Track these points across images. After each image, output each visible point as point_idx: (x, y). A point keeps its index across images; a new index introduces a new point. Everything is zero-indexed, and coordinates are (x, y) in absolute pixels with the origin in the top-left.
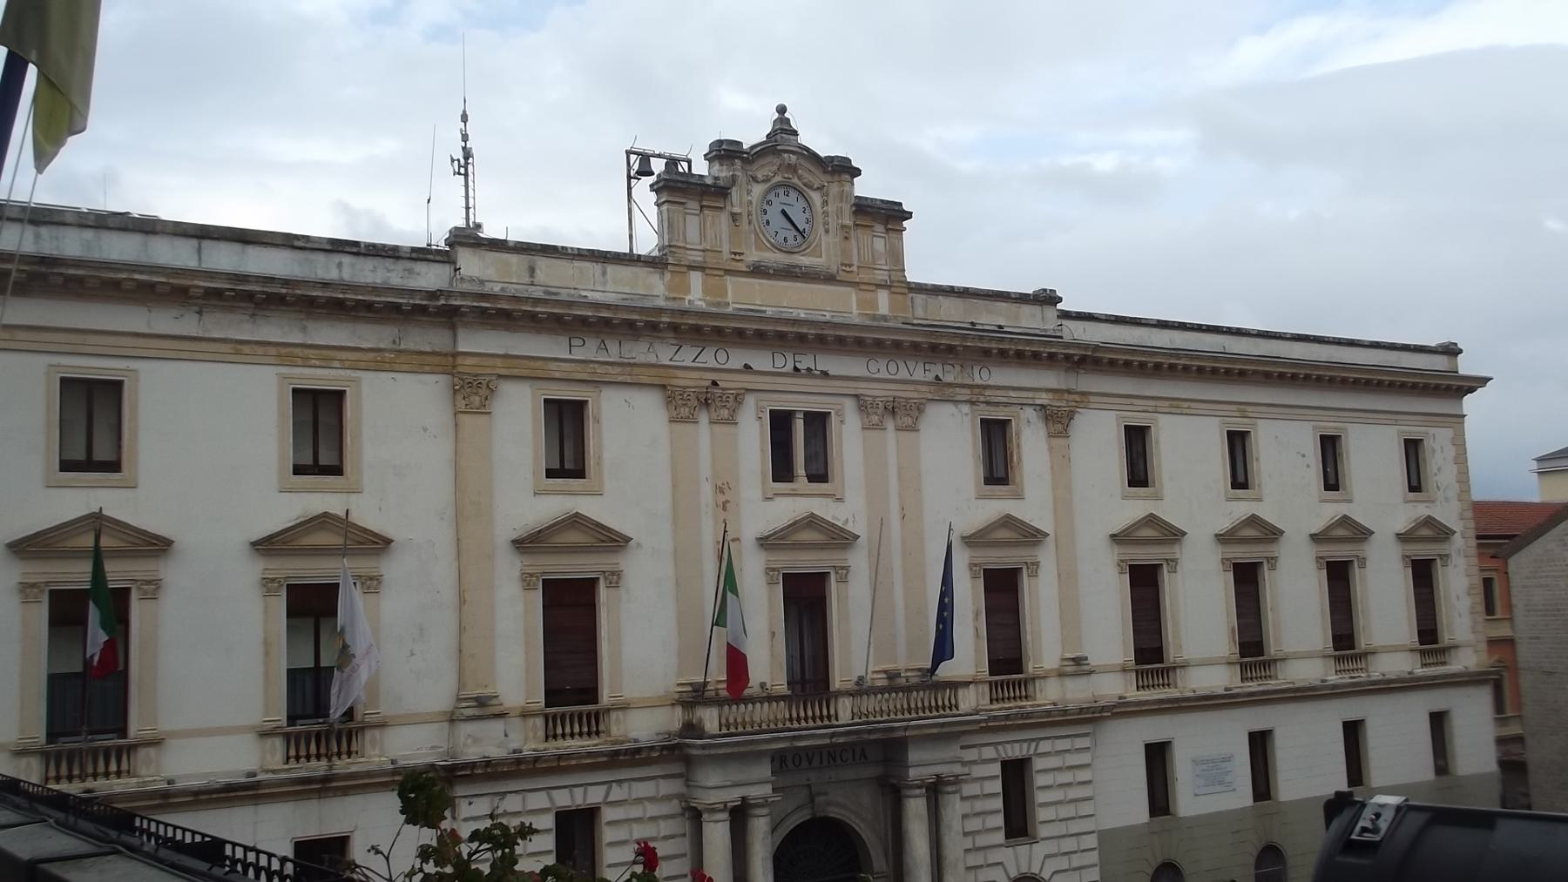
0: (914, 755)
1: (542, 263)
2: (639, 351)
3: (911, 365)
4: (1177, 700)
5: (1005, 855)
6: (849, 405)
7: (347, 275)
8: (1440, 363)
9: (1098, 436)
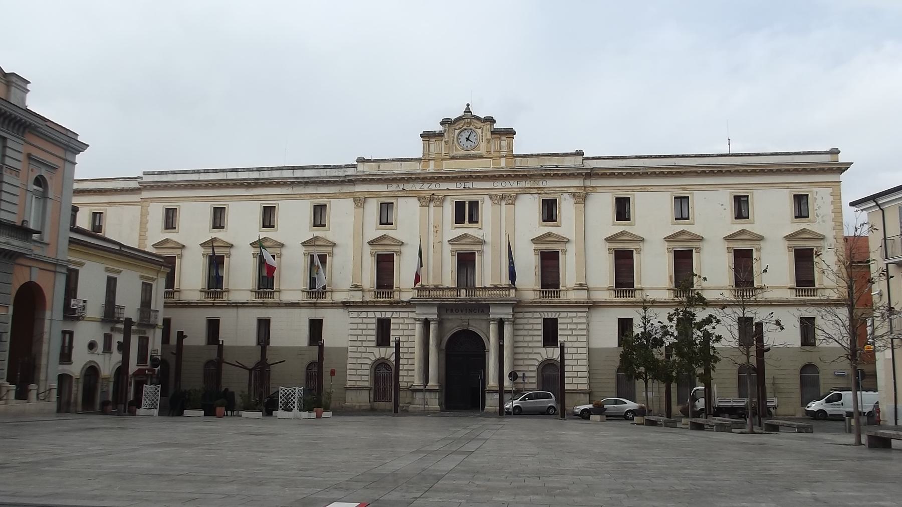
0: (491, 311)
1: (382, 164)
2: (409, 187)
3: (512, 182)
4: (633, 302)
5: (543, 351)
6: (487, 198)
7: (328, 174)
8: (827, 158)
9: (602, 204)
